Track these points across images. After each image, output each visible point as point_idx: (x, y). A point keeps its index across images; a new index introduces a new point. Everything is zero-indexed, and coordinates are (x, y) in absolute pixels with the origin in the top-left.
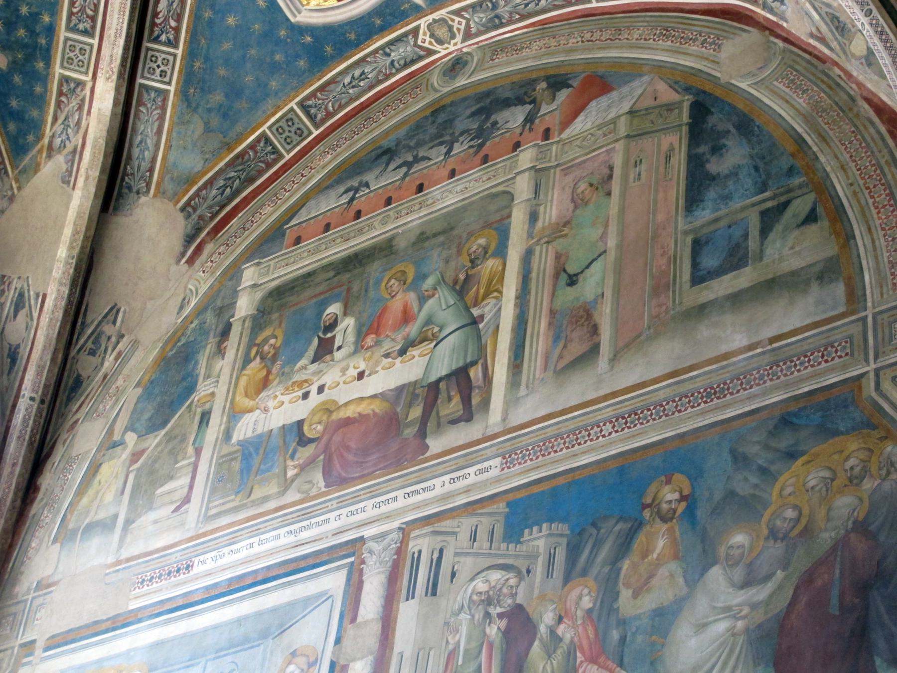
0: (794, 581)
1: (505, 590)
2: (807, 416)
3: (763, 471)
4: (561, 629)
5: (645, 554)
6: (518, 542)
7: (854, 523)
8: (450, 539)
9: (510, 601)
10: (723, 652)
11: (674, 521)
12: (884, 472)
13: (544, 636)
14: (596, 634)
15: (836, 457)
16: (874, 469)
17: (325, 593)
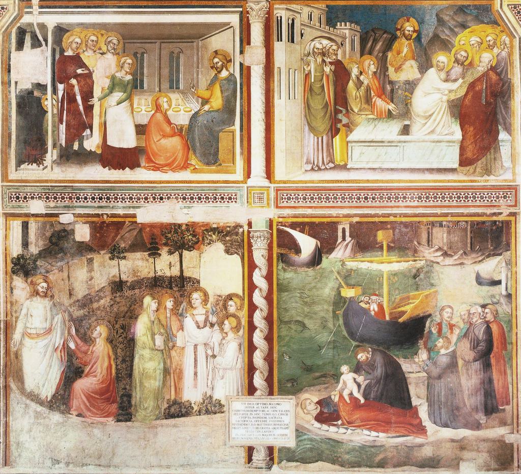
0: (467, 85)
1: (331, 50)
2: (471, 10)
3: (451, 30)
4: (362, 78)
5: (399, 53)
6: (335, 28)
7: (491, 66)
8: (298, 16)
9: (334, 57)
10: (437, 109)
11: (411, 40)
12: (502, 47)
13: (354, 79)
14: (379, 84)
15: (483, 33)
16: (498, 44)
17: (228, 24)
